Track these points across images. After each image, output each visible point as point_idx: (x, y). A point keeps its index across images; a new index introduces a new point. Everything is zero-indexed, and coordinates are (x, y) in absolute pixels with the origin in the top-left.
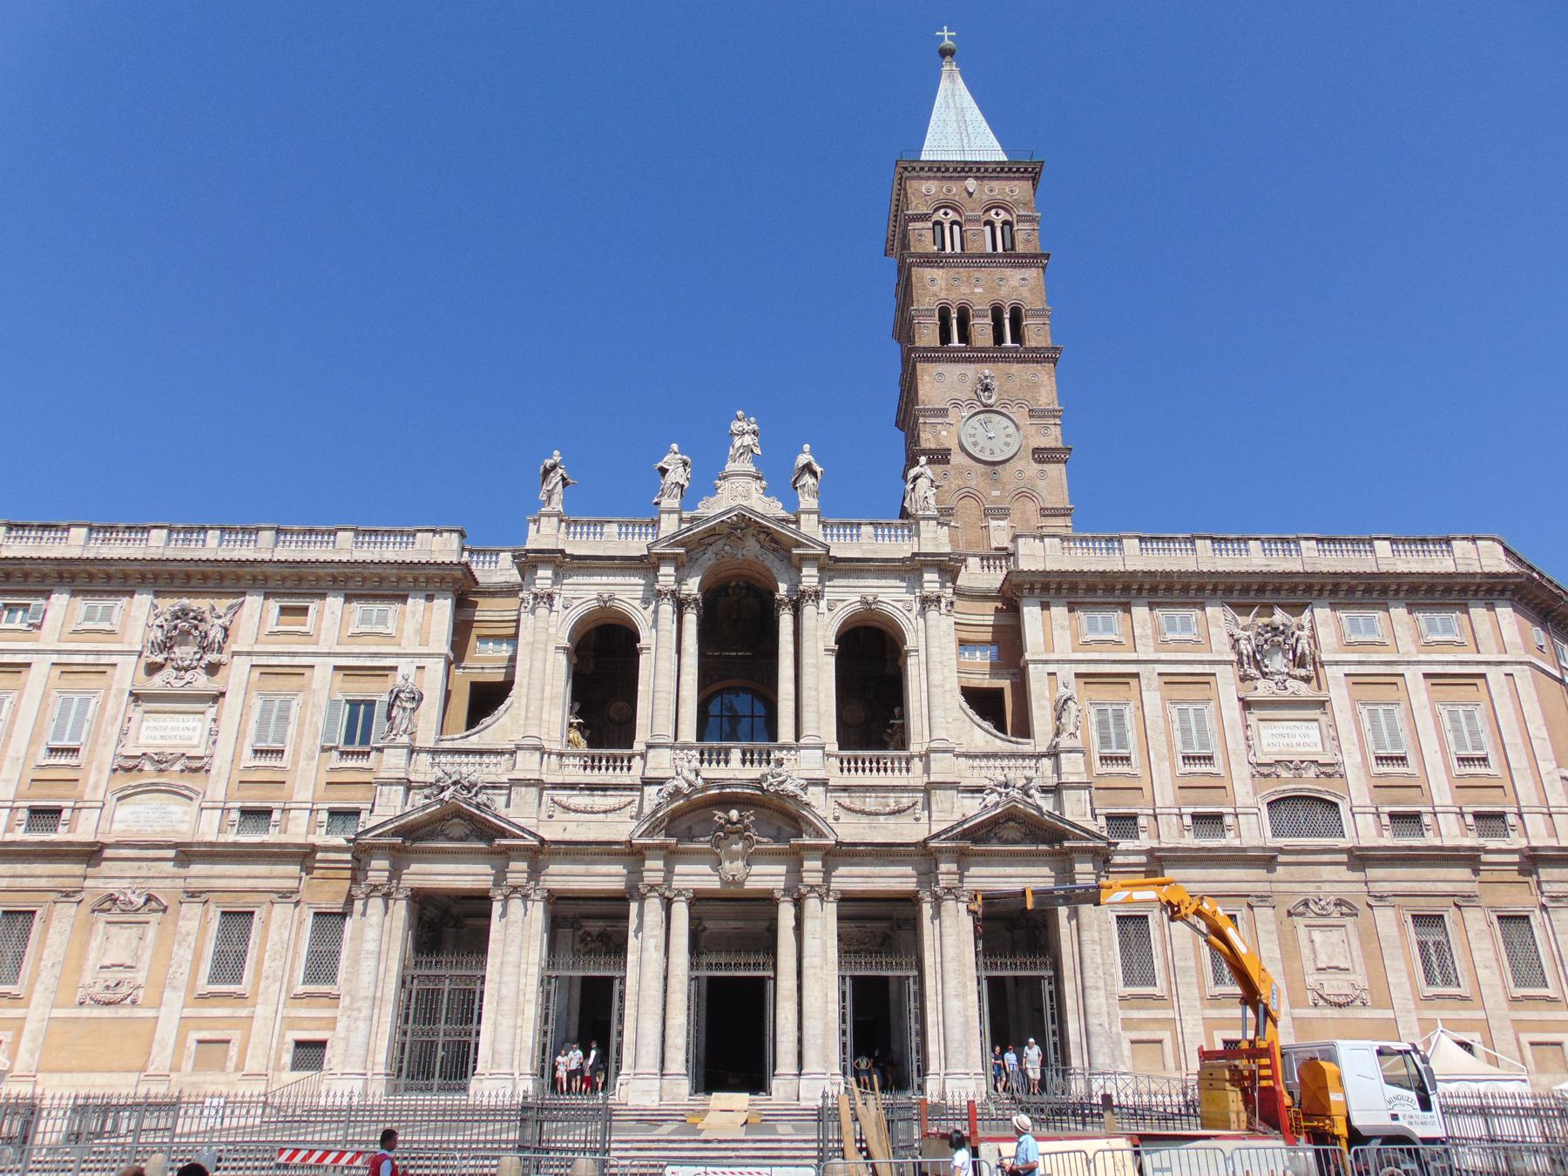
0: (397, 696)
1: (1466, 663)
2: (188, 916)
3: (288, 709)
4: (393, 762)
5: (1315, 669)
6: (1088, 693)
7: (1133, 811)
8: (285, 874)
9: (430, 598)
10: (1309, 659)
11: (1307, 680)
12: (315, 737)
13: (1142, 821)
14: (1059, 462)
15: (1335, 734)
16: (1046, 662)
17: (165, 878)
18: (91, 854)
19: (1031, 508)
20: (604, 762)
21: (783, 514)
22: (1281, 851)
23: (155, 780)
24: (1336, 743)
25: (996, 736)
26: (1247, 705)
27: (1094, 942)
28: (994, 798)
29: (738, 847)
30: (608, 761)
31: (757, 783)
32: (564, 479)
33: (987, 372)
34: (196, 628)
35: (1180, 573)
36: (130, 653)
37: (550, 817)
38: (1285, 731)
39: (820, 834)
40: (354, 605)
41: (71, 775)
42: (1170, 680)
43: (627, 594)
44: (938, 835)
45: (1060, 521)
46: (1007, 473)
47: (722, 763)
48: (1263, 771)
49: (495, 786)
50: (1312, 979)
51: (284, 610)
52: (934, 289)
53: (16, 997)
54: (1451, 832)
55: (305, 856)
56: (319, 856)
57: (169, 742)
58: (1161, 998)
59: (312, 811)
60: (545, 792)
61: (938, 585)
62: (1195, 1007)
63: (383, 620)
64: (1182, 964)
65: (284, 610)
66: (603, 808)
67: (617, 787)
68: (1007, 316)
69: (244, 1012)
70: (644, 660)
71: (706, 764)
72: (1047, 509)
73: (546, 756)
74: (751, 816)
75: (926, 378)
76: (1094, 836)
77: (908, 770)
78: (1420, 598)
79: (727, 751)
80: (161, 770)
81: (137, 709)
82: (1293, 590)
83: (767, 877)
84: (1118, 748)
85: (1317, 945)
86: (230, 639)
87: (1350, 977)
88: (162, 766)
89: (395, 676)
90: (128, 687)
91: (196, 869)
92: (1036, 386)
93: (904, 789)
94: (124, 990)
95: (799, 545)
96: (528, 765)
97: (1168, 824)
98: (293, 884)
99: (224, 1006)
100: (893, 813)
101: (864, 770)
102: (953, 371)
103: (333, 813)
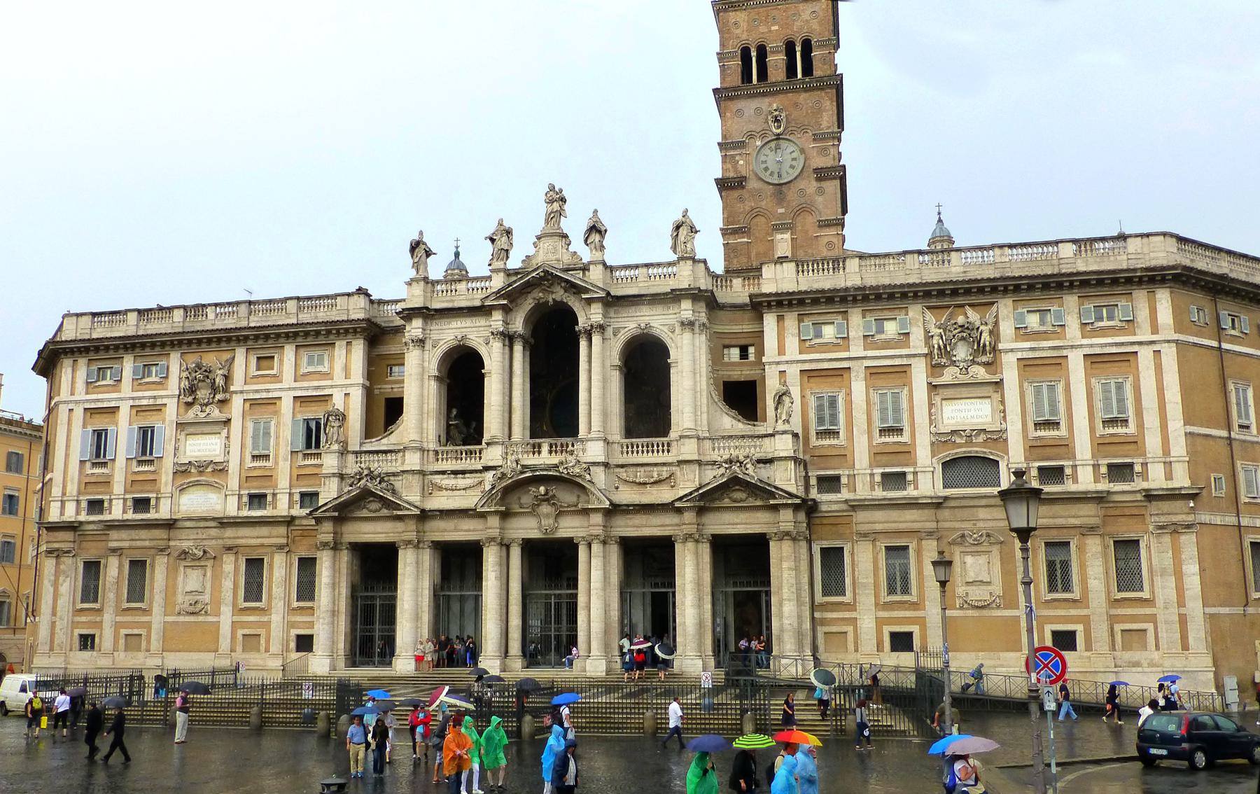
0: (328, 418)
1: (1122, 344)
2: (228, 562)
4: (330, 462)
5: (995, 355)
6: (810, 385)
7: (837, 473)
8: (278, 535)
10: (988, 348)
13: (844, 480)
14: (834, 178)
15: (1002, 408)
16: (778, 363)
18: (170, 525)
19: (810, 221)
22: (946, 498)
23: (199, 479)
24: (1002, 414)
25: (739, 421)
26: (933, 387)
27: (790, 569)
28: (722, 470)
30: (466, 454)
31: (556, 466)
32: (426, 251)
33: (775, 106)
34: (208, 377)
35: (884, 287)
36: (172, 396)
37: (431, 494)
38: (964, 407)
39: (601, 502)
40: (302, 351)
41: (151, 477)
42: (874, 373)
44: (680, 499)
45: (832, 231)
46: (792, 194)
47: (536, 454)
48: (941, 440)
49: (394, 474)
50: (961, 590)
51: (258, 358)
52: (738, 31)
53: (144, 610)
54: (1085, 480)
55: (290, 521)
56: (297, 522)
58: (848, 604)
59: (290, 494)
60: (427, 477)
61: (691, 312)
62: (871, 610)
63: (321, 362)
64: (865, 581)
66: (464, 486)
67: (471, 472)
68: (798, 49)
69: (265, 619)
70: (486, 380)
71: (525, 456)
72: (822, 221)
73: (426, 453)
74: (555, 490)
75: (728, 114)
76: (791, 495)
77: (668, 451)
78: (1092, 292)
79: (540, 446)
80: (201, 472)
81: (183, 433)
82: (981, 291)
83: (569, 528)
84: (830, 425)
85: (968, 565)
86: (230, 382)
87: (989, 588)
88: (201, 469)
90: (174, 418)
91: (229, 532)
92: (818, 112)
93: (664, 464)
94: (199, 606)
95: (586, 291)
96: (412, 461)
97: (863, 481)
98: (284, 541)
99: (254, 615)
100: (655, 483)
101: (638, 452)
102: (749, 107)
103: (303, 495)
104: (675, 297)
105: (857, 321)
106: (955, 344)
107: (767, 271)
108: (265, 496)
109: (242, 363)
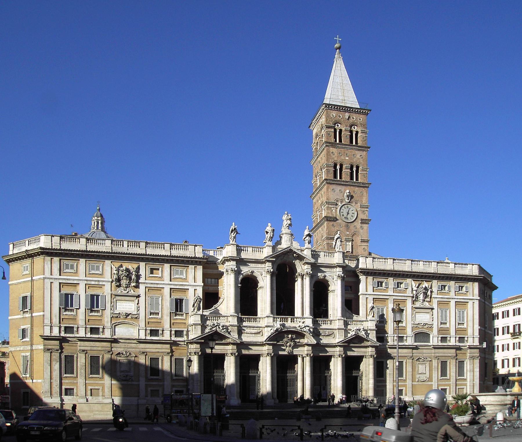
0: (196, 301)
3: (159, 301)
12: (168, 310)
16: (366, 294)
20: (252, 320)
21: (299, 248)
41: (99, 318)
48: (415, 326)
54: (452, 342)
57: (125, 310)
63: (182, 273)
79: (287, 319)
89: (188, 291)
105: (391, 282)
106: (421, 294)
107: (361, 260)
108: (158, 330)
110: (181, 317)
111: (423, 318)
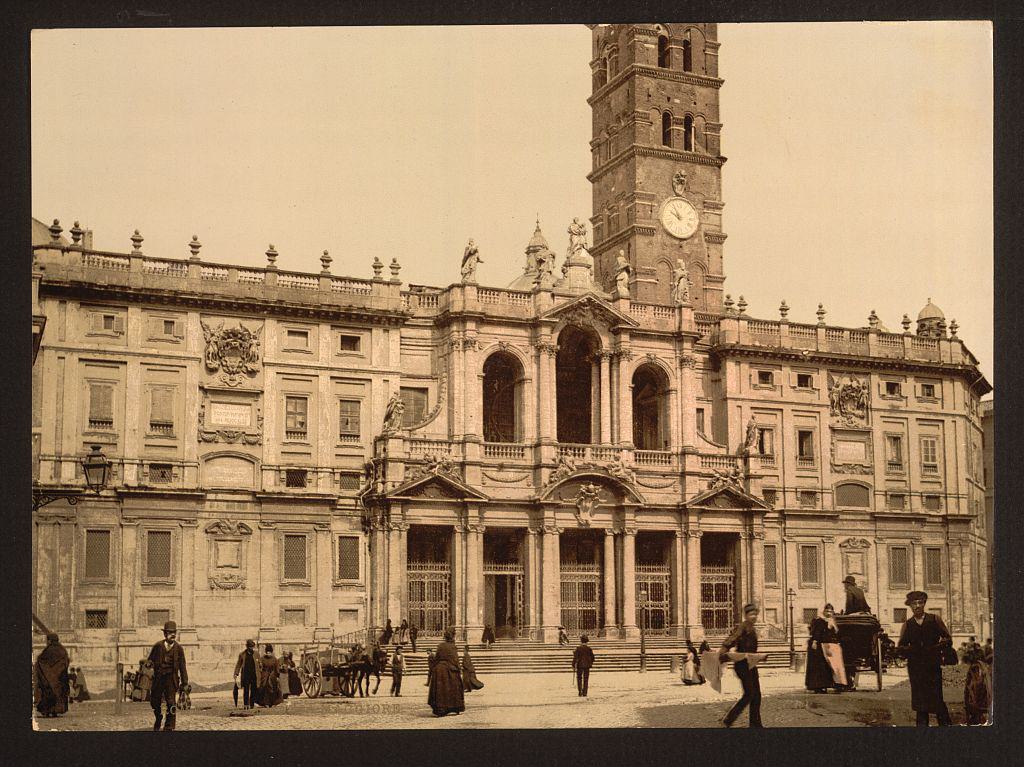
4: (395, 449)
9: (386, 331)
11: (862, 418)
16: (736, 399)
17: (251, 516)
18: (198, 496)
22: (843, 512)
26: (833, 430)
29: (589, 505)
43: (517, 342)
65: (291, 333)
74: (599, 489)
83: (601, 521)
96: (475, 453)
104: (678, 337)
109: (271, 337)
110: (353, 443)
111: (852, 451)
